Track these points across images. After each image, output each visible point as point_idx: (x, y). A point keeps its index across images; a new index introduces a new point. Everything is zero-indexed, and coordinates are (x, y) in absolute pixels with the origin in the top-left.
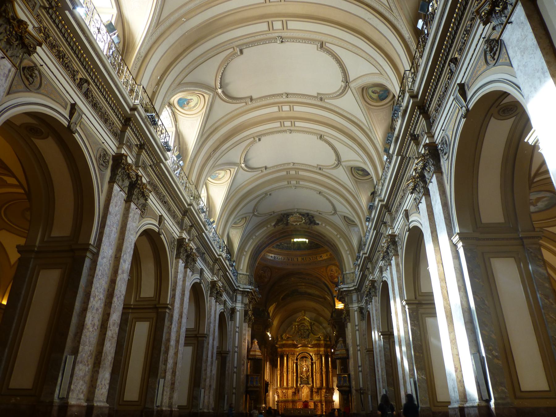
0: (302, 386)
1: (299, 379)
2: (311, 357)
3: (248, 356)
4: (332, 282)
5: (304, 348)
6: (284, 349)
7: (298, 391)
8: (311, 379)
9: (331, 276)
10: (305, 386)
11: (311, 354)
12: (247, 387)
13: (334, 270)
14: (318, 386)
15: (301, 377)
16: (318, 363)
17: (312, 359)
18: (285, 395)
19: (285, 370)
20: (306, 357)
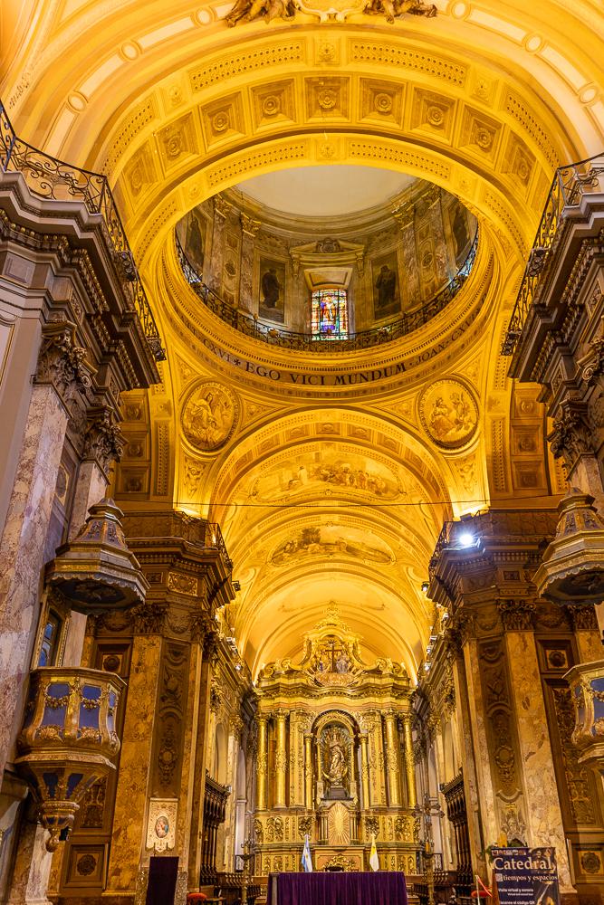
0: (328, 803)
1: (320, 784)
2: (355, 723)
3: (48, 568)
4: (439, 443)
5: (335, 699)
6: (277, 700)
7: (319, 819)
8: (353, 785)
9: (436, 425)
10: (339, 803)
11: (354, 715)
12: (22, 748)
13: (447, 401)
14: (379, 802)
15: (326, 781)
16: (376, 737)
17: (356, 731)
18: (279, 831)
19: (281, 759)
20: (342, 726)
